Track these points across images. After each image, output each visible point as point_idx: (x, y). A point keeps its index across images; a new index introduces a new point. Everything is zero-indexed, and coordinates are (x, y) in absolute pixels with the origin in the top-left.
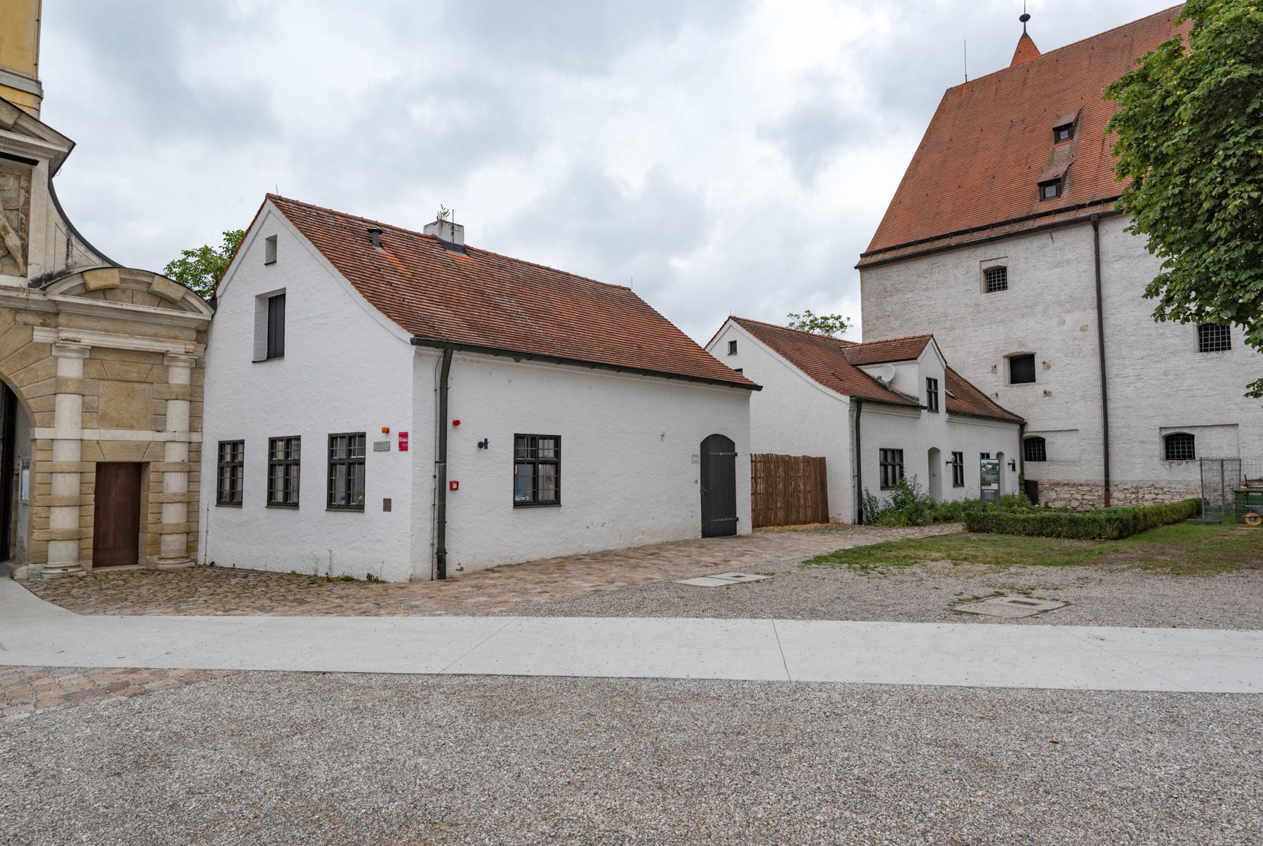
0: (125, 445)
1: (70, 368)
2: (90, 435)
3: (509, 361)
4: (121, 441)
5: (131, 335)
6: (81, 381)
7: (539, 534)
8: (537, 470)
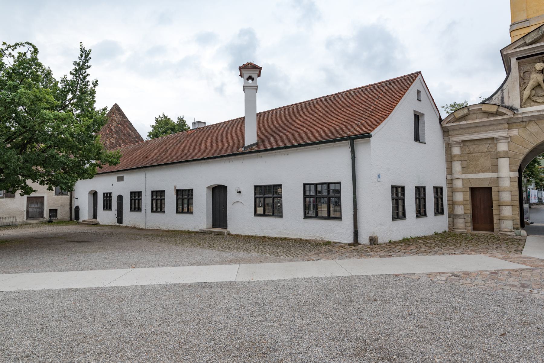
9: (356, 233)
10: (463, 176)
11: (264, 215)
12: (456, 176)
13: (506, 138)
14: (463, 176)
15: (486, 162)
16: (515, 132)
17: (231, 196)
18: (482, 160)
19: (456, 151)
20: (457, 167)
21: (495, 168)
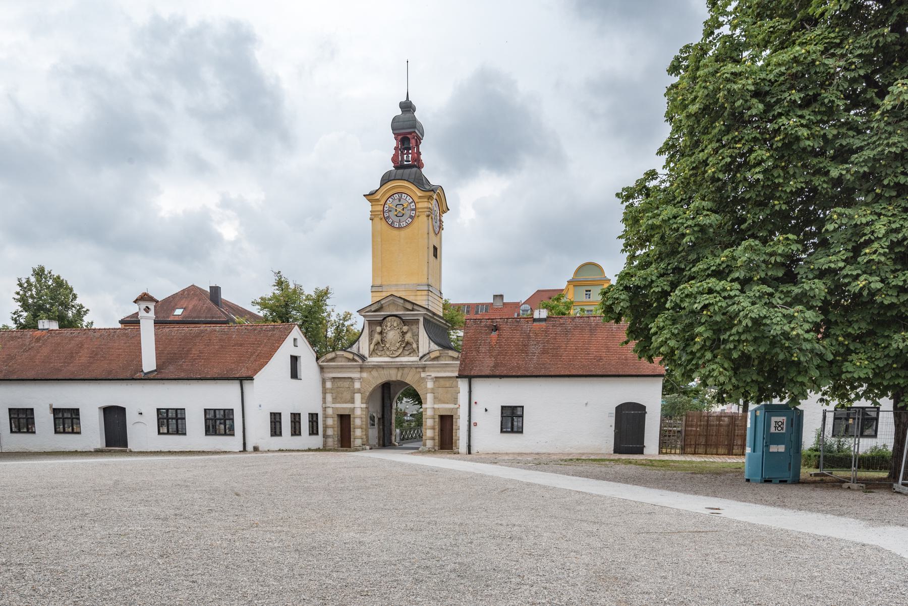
0: (446, 409)
1: (430, 385)
2: (436, 406)
3: (498, 379)
4: (445, 408)
5: (445, 371)
6: (432, 389)
7: (512, 443)
8: (512, 419)
9: (244, 444)
10: (333, 405)
11: (168, 433)
12: (328, 405)
13: (359, 379)
14: (333, 405)
15: (347, 395)
16: (365, 375)
17: (131, 417)
18: (345, 393)
19: (329, 385)
20: (329, 397)
21: (352, 401)
